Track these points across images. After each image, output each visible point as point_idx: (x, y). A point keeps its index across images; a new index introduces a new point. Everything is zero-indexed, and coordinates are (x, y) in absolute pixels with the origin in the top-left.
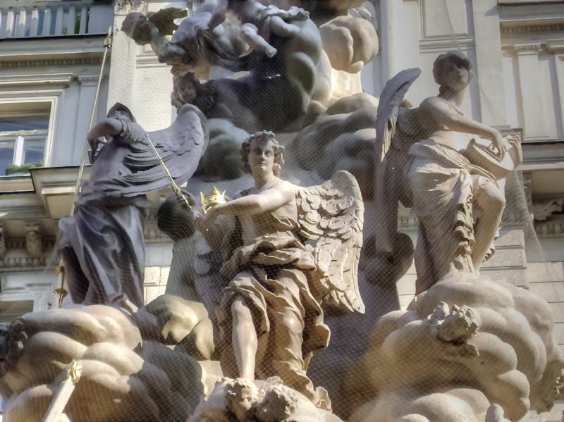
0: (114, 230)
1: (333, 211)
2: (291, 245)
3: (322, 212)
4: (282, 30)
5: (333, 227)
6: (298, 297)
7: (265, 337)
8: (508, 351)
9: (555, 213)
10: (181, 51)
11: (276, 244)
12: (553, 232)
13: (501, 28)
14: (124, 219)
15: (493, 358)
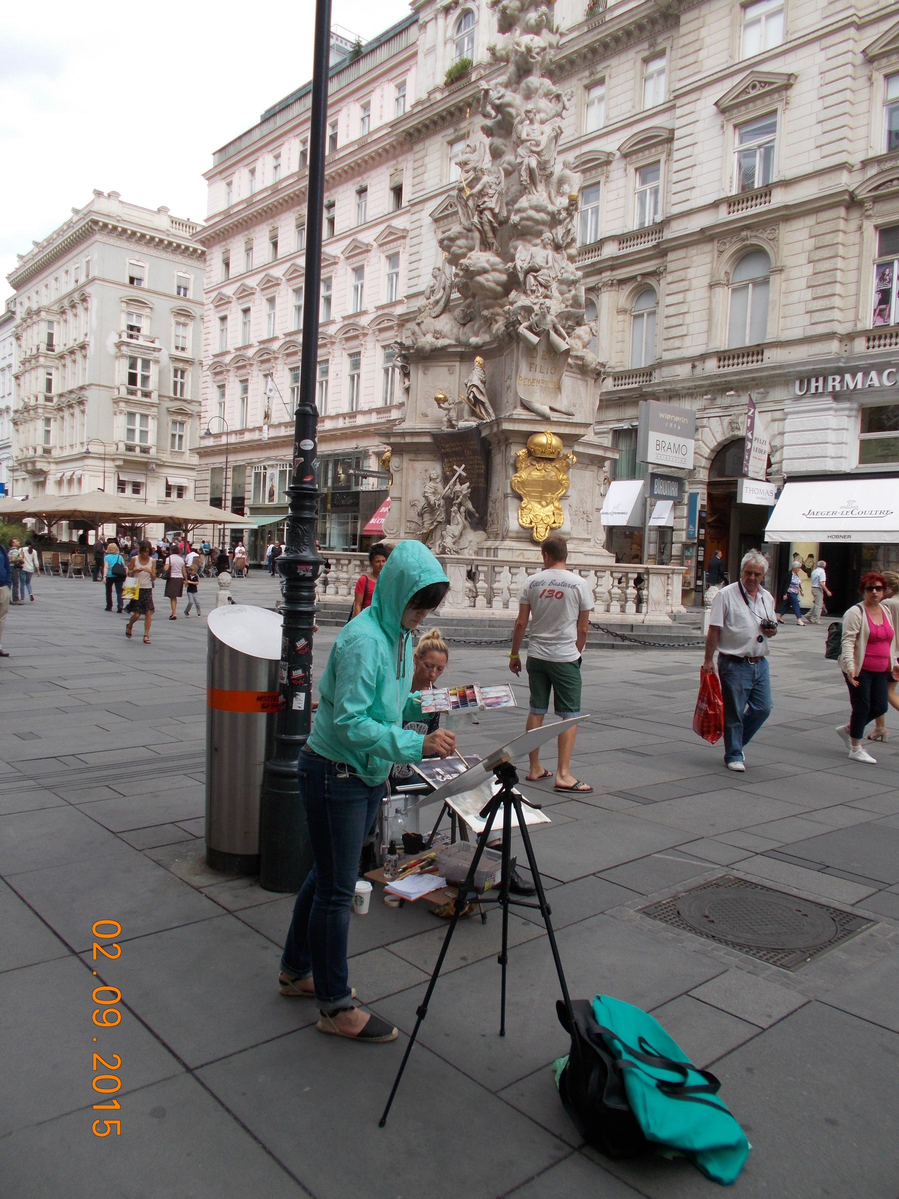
8: (529, 223)
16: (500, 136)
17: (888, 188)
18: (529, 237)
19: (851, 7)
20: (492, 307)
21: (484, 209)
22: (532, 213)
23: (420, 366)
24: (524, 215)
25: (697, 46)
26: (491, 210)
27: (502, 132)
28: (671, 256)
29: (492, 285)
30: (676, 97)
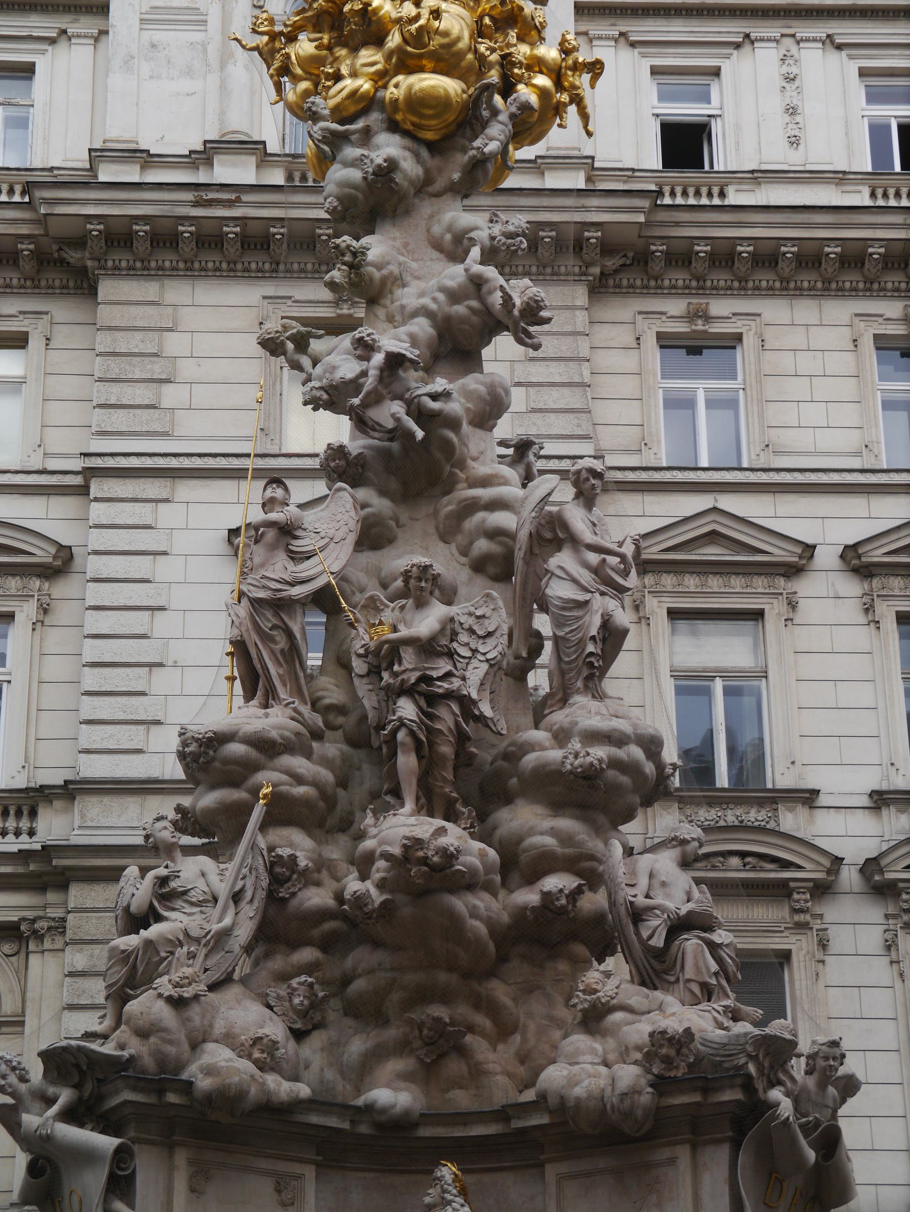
0: (283, 629)
1: (480, 633)
2: (448, 675)
3: (471, 631)
4: (432, 410)
5: (482, 649)
6: (452, 727)
7: (424, 761)
8: (625, 780)
9: (624, 265)
10: (325, 396)
11: (435, 674)
12: (619, 286)
13: (575, 7)
14: (290, 618)
15: (615, 789)
16: (383, 492)
17: (714, 868)
18: (602, 819)
19: (586, 437)
20: (445, 997)
21: (450, 695)
22: (636, 752)
23: (181, 1158)
24: (619, 753)
25: (157, 369)
26: (466, 704)
27: (394, 484)
28: (78, 895)
29: (481, 928)
30: (90, 473)
